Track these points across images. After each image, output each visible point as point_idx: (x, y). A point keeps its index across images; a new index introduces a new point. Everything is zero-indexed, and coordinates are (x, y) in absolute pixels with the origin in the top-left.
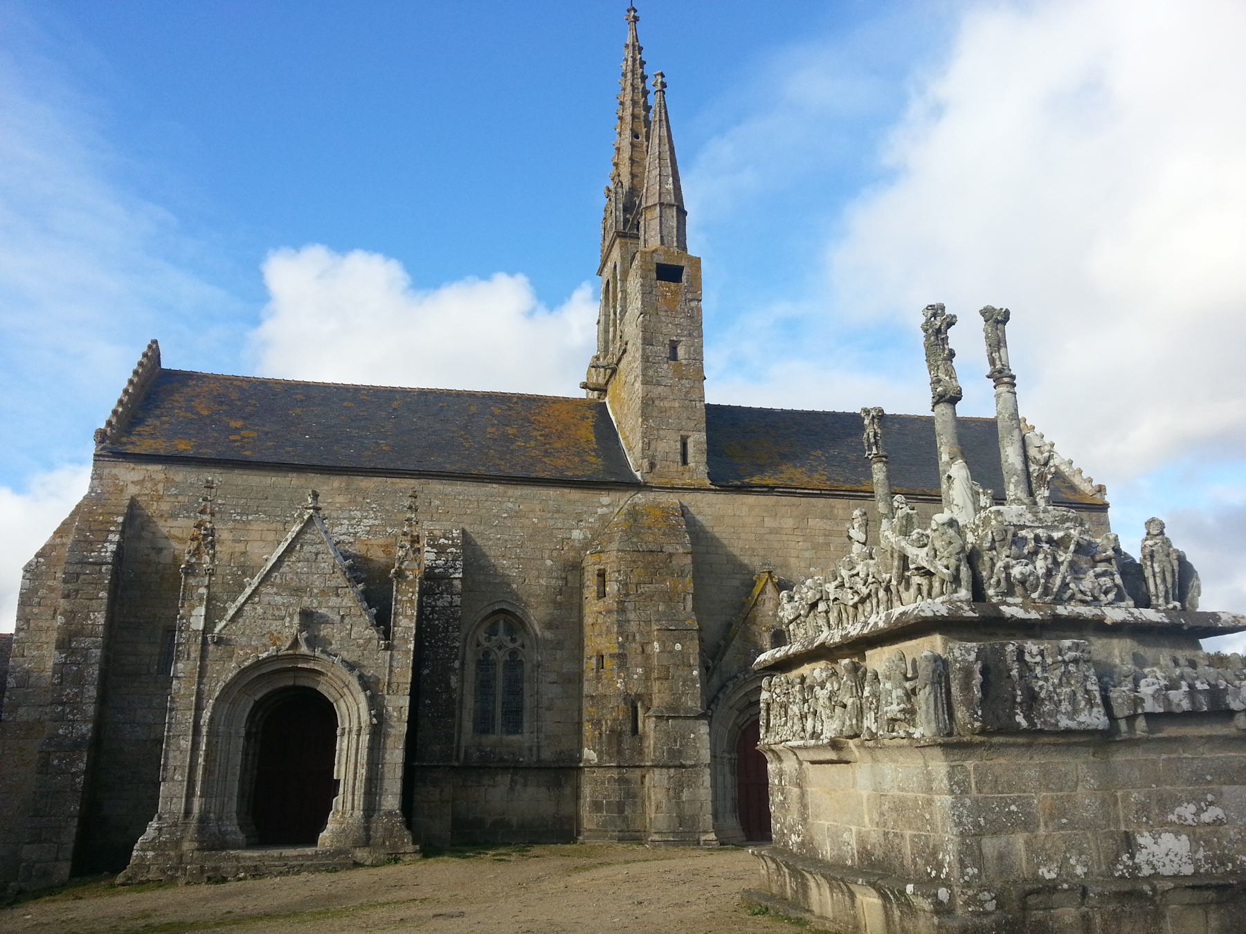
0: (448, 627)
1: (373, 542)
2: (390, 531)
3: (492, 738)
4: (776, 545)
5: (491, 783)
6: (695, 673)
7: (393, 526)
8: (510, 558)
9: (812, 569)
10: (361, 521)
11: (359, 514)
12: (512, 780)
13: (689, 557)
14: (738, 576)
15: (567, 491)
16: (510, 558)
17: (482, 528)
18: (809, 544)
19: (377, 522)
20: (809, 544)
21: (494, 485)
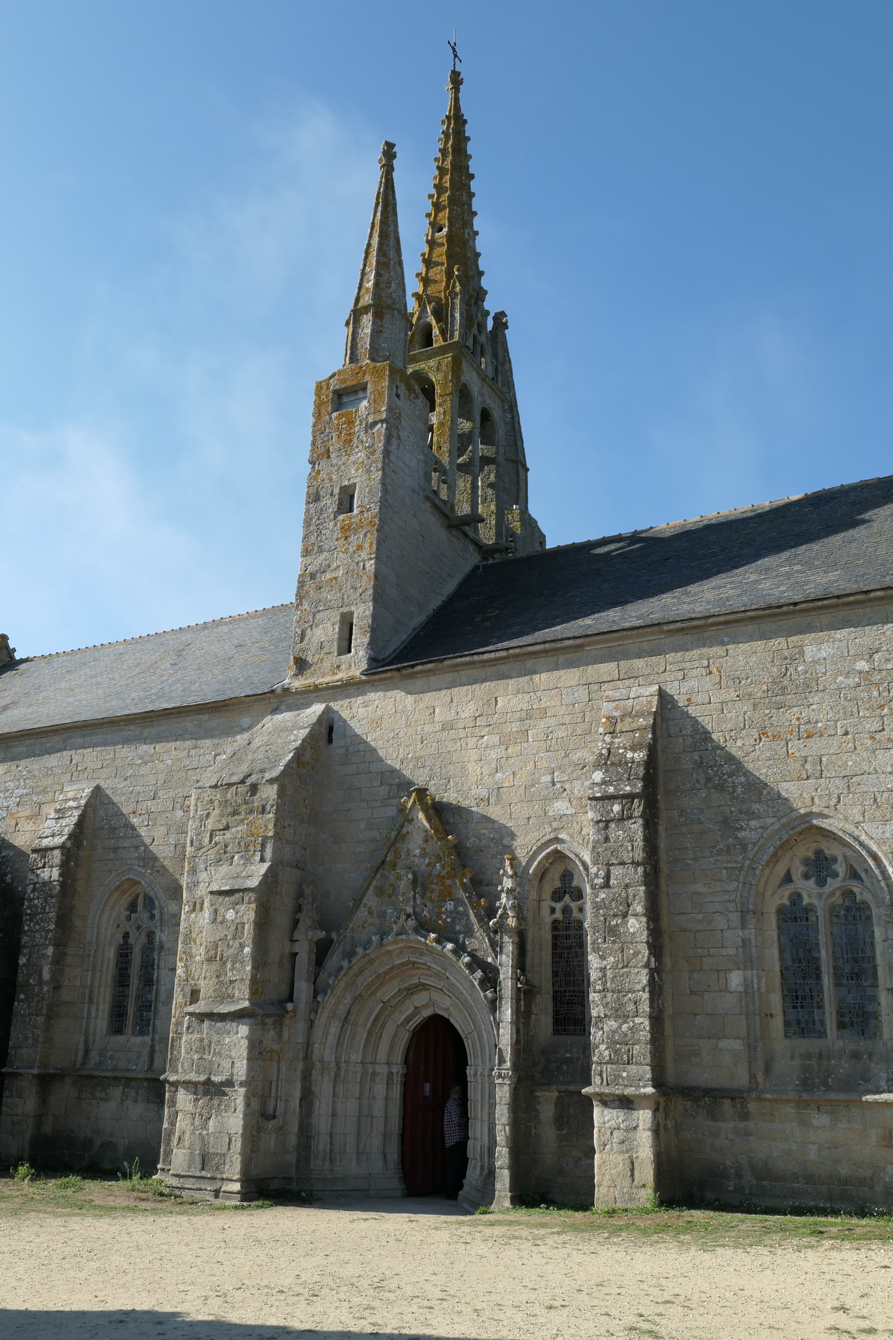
0: (46, 906)
1: (21, 814)
2: (35, 799)
3: (120, 1038)
4: (451, 746)
5: (103, 1095)
6: (247, 950)
7: (37, 794)
8: (140, 815)
10: (12, 793)
11: (11, 785)
12: (123, 1093)
13: (275, 787)
15: (205, 717)
16: (140, 815)
17: (116, 781)
18: (496, 739)
19: (25, 791)
20: (496, 739)
21: (131, 728)
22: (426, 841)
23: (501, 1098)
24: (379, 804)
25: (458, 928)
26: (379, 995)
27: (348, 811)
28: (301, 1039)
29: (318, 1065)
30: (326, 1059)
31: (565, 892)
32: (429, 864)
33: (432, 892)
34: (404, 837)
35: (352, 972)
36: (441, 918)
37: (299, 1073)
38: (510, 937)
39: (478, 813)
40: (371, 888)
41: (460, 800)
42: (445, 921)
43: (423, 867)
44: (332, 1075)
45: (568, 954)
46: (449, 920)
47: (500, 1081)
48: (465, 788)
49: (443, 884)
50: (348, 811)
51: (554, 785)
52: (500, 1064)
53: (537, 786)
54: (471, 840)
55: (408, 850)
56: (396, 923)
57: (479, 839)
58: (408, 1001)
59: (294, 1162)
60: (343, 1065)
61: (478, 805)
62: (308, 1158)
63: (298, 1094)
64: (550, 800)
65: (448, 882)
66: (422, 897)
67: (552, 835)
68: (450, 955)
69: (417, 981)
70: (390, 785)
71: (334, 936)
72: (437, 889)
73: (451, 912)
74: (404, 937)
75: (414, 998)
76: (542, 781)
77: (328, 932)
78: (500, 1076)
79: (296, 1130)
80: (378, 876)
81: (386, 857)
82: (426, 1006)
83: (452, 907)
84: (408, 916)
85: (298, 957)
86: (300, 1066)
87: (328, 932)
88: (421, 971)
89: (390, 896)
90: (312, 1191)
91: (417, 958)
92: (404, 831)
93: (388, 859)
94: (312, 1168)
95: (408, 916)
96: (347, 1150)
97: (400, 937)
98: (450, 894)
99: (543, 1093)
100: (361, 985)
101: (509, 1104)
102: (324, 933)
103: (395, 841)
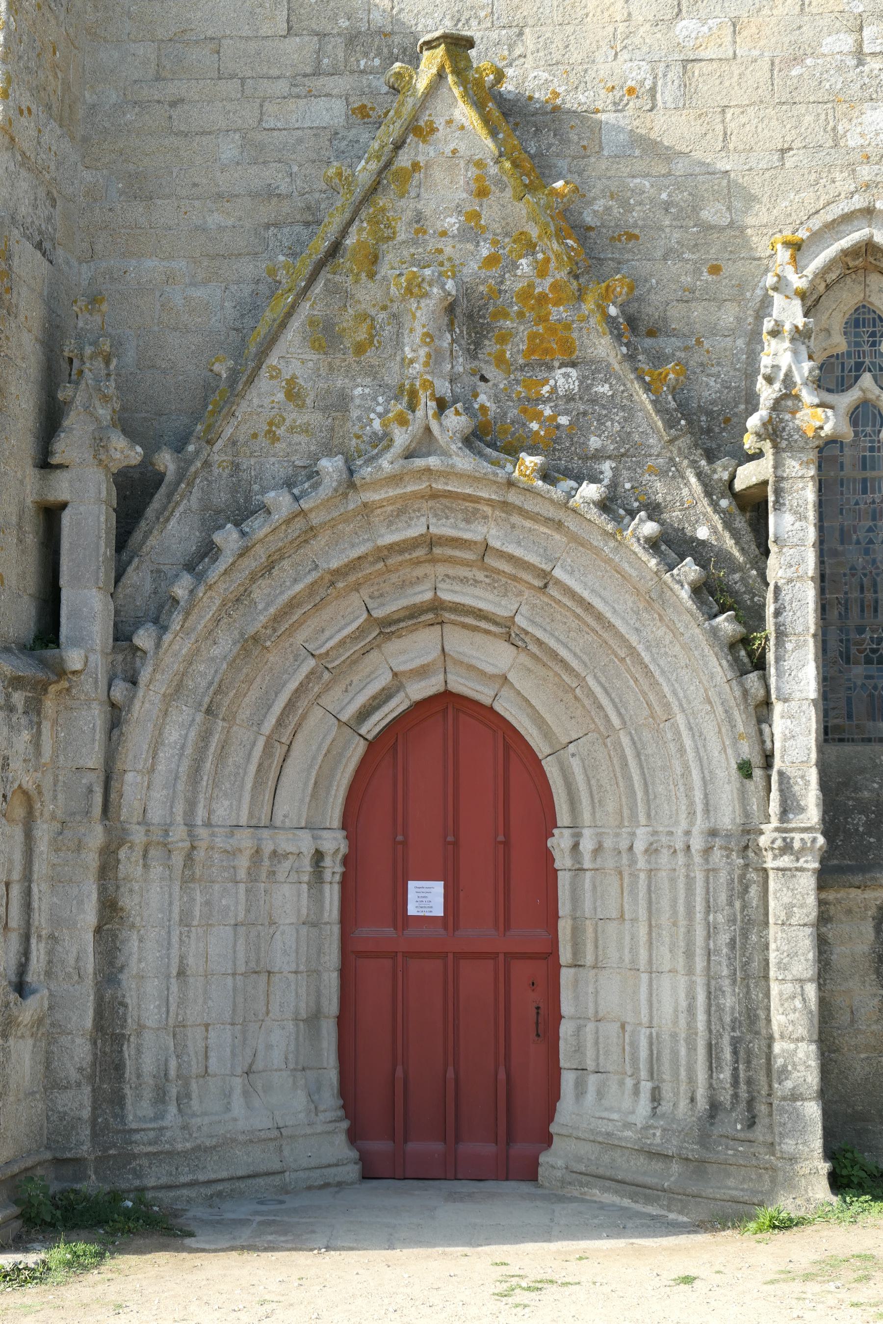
9: (686, 27)
14: (340, 84)
22: (482, 193)
23: (789, 909)
24: (282, 87)
25: (594, 442)
26: (300, 637)
27: (173, 104)
28: (93, 758)
29: (138, 836)
30: (156, 815)
31: (859, 366)
32: (491, 261)
33: (503, 339)
34: (404, 177)
35: (250, 564)
36: (538, 416)
37: (92, 859)
38: (805, 464)
39: (619, 129)
40: (296, 323)
41: (561, 90)
42: (551, 424)
43: (473, 266)
44: (178, 859)
45: (870, 530)
46: (563, 420)
47: (786, 861)
48: (576, 56)
49: (543, 319)
50: (173, 104)
51: (861, 63)
52: (784, 813)
53: (809, 61)
54: (599, 205)
55: (419, 217)
56: (402, 421)
57: (624, 204)
58: (374, 655)
59: (86, 1113)
60: (202, 832)
61: (618, 107)
62: (118, 1100)
63: (90, 917)
64: (851, 103)
65: (558, 313)
66: (473, 355)
67: (858, 202)
68: (594, 514)
69: (428, 596)
70: (322, 36)
71: (166, 461)
72: (523, 331)
73: (570, 398)
74: (433, 461)
75: (393, 646)
76: (825, 50)
77: (151, 449)
78: (787, 848)
79: (89, 1023)
80: (318, 288)
81: (344, 232)
82: (422, 672)
83: (575, 387)
84: (442, 405)
85: (67, 519)
86: (96, 837)
87: (151, 449)
88: (441, 569)
89: (360, 349)
90: (142, 1190)
91: (455, 527)
92: (404, 160)
93: (350, 241)
94: (134, 1126)
95: (442, 405)
96: (213, 1068)
97: (419, 463)
98: (567, 347)
99: (841, 894)
100: (268, 605)
101: (813, 925)
102: (139, 449)
103: (375, 188)
